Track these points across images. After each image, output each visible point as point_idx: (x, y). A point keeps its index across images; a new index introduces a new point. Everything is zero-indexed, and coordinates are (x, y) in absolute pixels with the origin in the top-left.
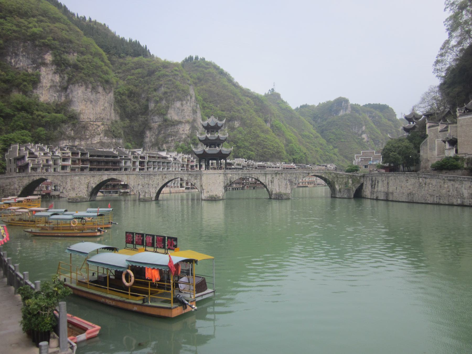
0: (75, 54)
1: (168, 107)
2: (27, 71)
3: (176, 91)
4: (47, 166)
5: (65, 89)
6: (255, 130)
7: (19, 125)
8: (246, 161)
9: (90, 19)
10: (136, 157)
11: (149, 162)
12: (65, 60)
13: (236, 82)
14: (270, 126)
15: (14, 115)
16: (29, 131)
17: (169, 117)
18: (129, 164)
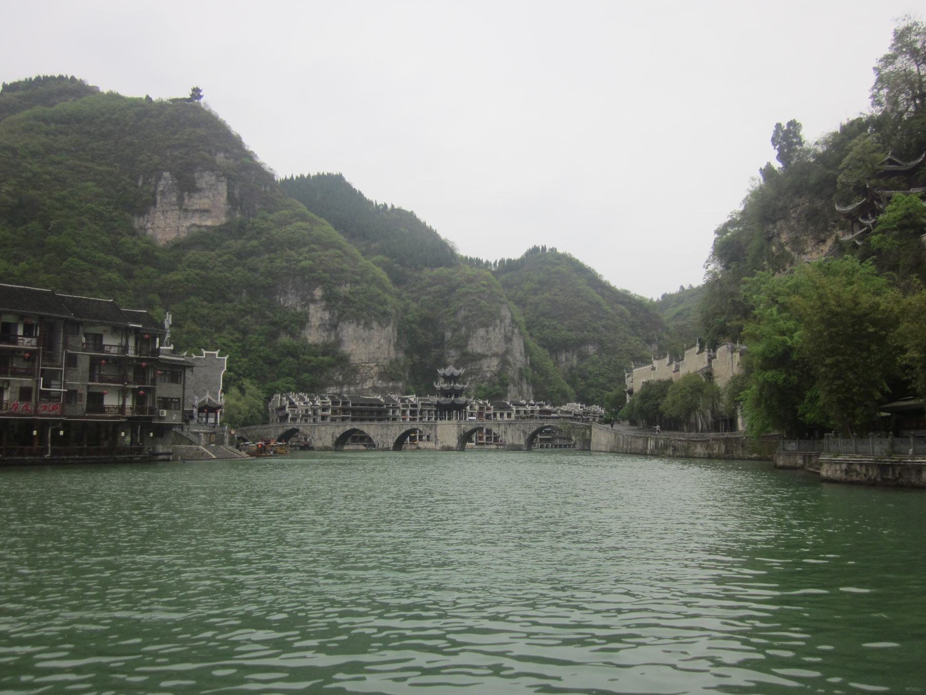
0: (348, 285)
4: (306, 417)
5: (335, 326)
6: (620, 358)
8: (581, 407)
9: (393, 206)
10: (407, 406)
11: (421, 411)
13: (606, 282)
15: (280, 361)
16: (294, 378)
17: (469, 349)
18: (398, 413)
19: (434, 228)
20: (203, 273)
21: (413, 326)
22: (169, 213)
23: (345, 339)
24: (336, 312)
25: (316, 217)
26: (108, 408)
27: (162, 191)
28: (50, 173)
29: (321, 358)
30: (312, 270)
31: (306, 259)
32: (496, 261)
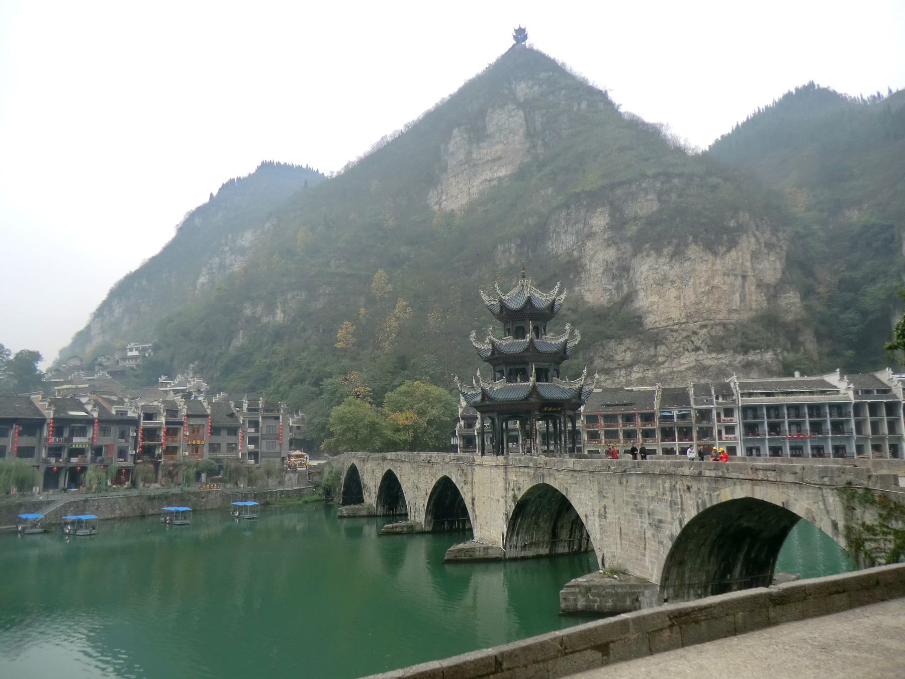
5: (625, 270)
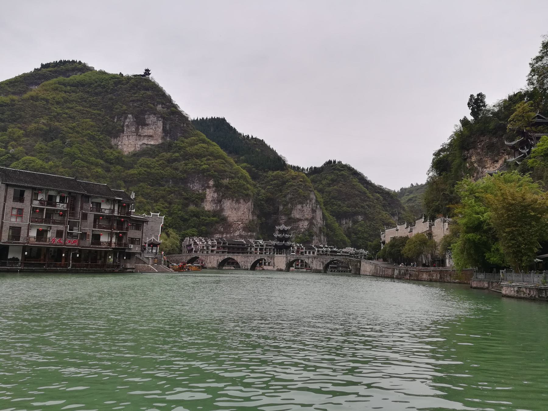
1: (292, 209)
2: (199, 192)
3: (299, 197)
4: (202, 250)
7: (191, 225)
8: (354, 250)
9: (252, 136)
10: (258, 246)
11: (266, 249)
12: (221, 184)
14: (397, 219)
15: (189, 219)
17: (292, 215)
18: (253, 250)
19: (274, 149)
20: (149, 170)
21: (262, 202)
22: (131, 137)
23: (225, 208)
24: (221, 193)
25: (211, 142)
26: (103, 243)
27: (127, 125)
28: (66, 114)
29: (212, 218)
30: (208, 170)
31: (205, 164)
32: (308, 168)
